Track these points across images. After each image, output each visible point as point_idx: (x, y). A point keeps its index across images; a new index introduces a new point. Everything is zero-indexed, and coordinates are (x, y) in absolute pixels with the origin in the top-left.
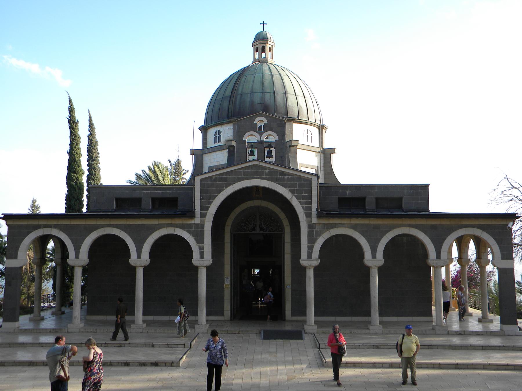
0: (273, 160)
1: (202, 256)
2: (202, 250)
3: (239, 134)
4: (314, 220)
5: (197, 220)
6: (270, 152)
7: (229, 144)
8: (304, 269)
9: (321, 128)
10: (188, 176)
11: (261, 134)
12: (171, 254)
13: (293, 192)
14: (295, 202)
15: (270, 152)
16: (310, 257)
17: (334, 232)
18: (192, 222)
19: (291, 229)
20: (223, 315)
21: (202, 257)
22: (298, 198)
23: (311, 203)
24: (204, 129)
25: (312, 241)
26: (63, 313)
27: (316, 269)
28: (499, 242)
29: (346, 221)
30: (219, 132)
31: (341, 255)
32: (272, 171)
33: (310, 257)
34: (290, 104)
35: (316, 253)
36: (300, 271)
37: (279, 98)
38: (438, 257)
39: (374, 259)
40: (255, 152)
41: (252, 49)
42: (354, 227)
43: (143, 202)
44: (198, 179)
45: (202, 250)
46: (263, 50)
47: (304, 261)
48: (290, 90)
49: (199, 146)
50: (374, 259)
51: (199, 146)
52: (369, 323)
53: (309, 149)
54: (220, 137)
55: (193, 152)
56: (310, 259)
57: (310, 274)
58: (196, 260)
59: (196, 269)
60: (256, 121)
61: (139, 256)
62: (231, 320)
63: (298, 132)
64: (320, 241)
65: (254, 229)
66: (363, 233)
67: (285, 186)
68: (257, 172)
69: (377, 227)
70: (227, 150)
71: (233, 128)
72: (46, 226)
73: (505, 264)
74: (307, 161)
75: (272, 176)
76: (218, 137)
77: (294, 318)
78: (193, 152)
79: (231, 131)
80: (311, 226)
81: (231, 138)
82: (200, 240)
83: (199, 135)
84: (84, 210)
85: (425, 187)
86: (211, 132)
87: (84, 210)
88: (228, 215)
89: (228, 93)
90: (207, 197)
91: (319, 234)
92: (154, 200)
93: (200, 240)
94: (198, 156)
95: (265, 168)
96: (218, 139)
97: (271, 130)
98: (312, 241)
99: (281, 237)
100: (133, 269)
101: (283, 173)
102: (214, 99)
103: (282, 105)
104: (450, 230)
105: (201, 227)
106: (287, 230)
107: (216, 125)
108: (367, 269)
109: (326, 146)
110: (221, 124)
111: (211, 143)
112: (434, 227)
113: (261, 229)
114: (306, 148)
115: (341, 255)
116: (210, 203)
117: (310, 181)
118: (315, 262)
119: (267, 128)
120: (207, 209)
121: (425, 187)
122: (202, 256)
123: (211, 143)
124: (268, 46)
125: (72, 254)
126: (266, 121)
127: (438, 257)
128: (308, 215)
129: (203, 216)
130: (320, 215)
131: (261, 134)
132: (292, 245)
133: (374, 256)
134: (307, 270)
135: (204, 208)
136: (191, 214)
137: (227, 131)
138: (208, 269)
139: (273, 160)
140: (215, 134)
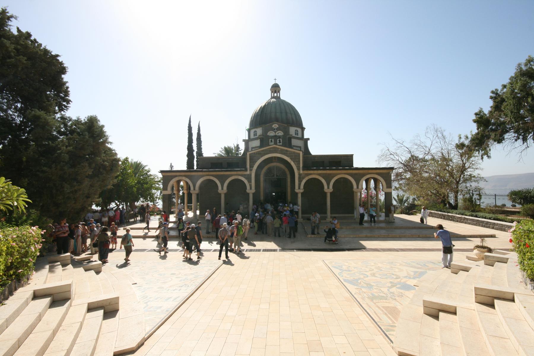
0: (281, 144)
1: (251, 189)
2: (251, 186)
3: (265, 132)
4: (301, 172)
5: (248, 172)
6: (280, 141)
8: (297, 194)
10: (242, 152)
11: (275, 132)
13: (291, 159)
14: (292, 164)
15: (280, 141)
16: (299, 188)
17: (310, 177)
21: (251, 190)
22: (294, 162)
23: (300, 164)
24: (249, 131)
28: (386, 181)
29: (316, 172)
32: (282, 150)
33: (299, 188)
35: (302, 187)
38: (358, 187)
39: (328, 189)
40: (273, 140)
41: (270, 92)
42: (319, 175)
44: (248, 154)
45: (251, 186)
47: (297, 190)
48: (288, 111)
49: (247, 138)
50: (328, 189)
51: (247, 138)
52: (326, 217)
55: (244, 140)
56: (299, 189)
58: (248, 190)
59: (248, 194)
60: (273, 126)
61: (222, 189)
64: (304, 181)
65: (274, 176)
67: (288, 156)
68: (275, 150)
69: (330, 174)
70: (259, 140)
73: (388, 190)
75: (282, 152)
78: (244, 140)
80: (300, 175)
82: (250, 181)
84: (195, 167)
85: (351, 156)
86: (252, 131)
87: (195, 167)
88: (262, 169)
89: (260, 113)
90: (253, 160)
91: (303, 178)
92: (228, 163)
93: (250, 181)
94: (246, 142)
95: (279, 148)
96: (255, 134)
97: (280, 130)
99: (285, 180)
100: (220, 194)
101: (287, 151)
104: (364, 175)
105: (250, 175)
107: (254, 128)
108: (325, 194)
109: (305, 137)
112: (356, 174)
117: (299, 154)
118: (302, 191)
119: (278, 129)
120: (253, 167)
121: (351, 156)
122: (251, 189)
123: (252, 136)
125: (192, 188)
126: (278, 126)
127: (358, 187)
129: (251, 170)
130: (303, 170)
131: (275, 132)
132: (291, 183)
133: (328, 188)
135: (251, 167)
136: (246, 170)
137: (259, 131)
138: (254, 194)
139: (281, 144)
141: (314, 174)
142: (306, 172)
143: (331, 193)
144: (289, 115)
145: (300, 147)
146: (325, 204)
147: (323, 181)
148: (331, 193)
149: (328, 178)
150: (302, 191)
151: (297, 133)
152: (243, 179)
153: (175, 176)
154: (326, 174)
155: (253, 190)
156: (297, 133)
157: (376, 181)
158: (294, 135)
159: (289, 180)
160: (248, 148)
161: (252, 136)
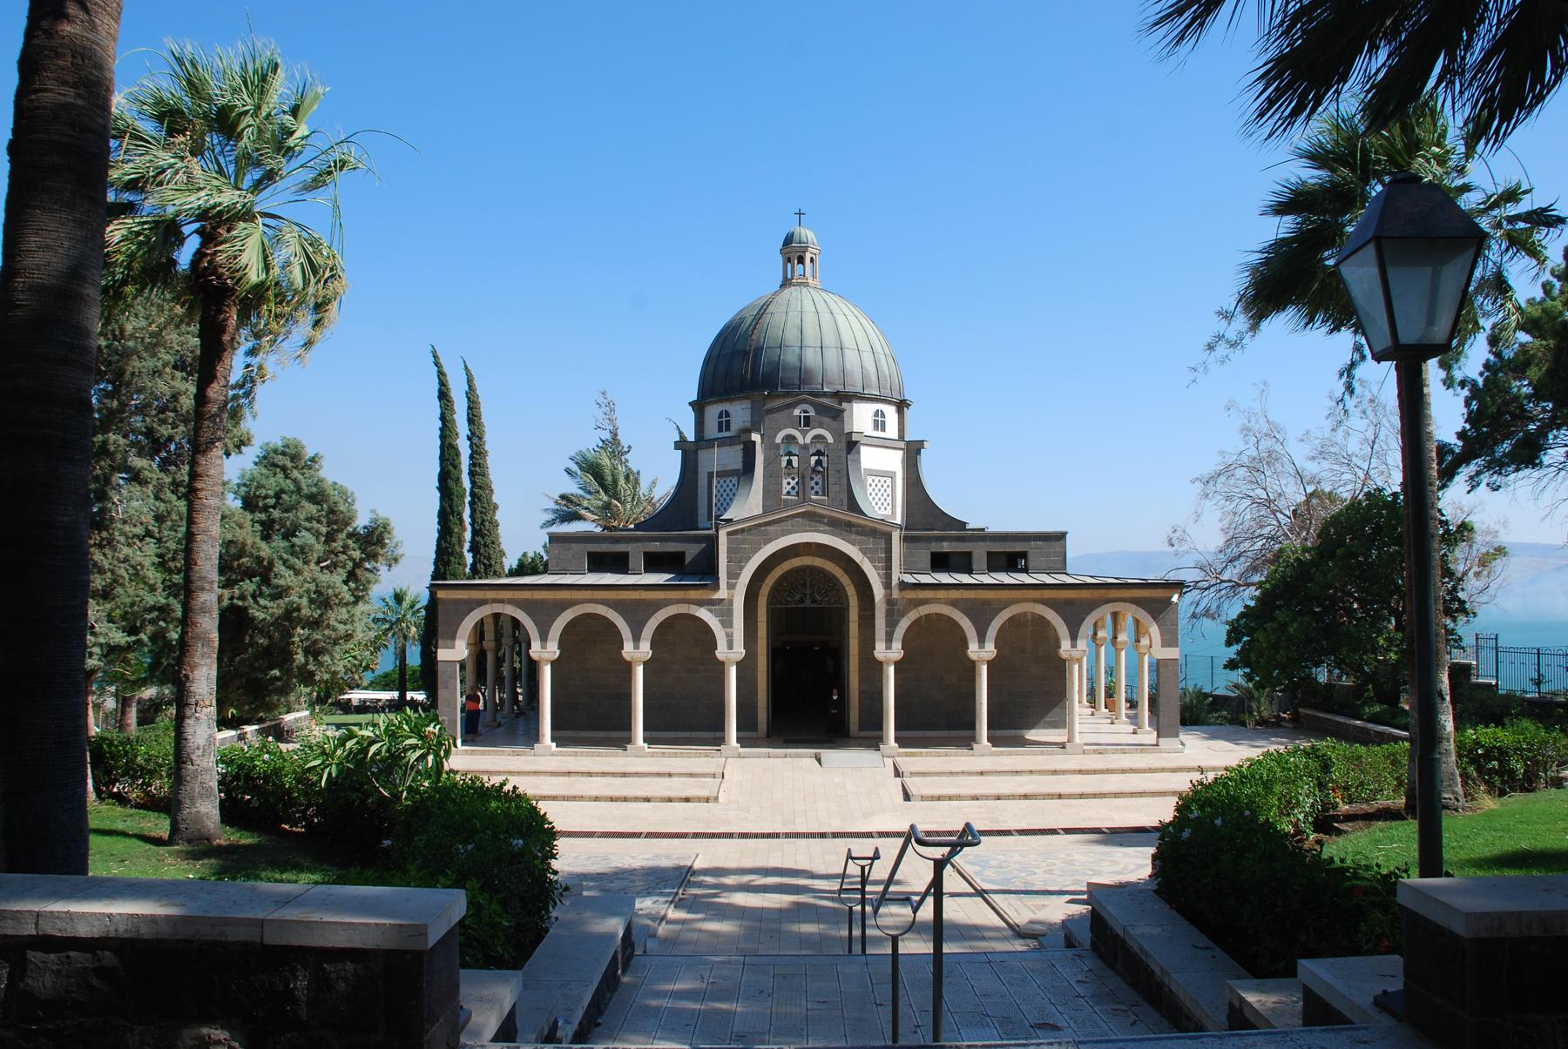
1: (730, 646)
4: (896, 594)
5: (722, 593)
7: (744, 438)
9: (902, 406)
12: (685, 645)
13: (864, 551)
17: (924, 610)
18: (716, 596)
19: (860, 599)
20: (755, 729)
21: (730, 647)
22: (872, 561)
24: (698, 407)
26: (499, 725)
29: (942, 594)
30: (727, 414)
34: (848, 366)
36: (873, 669)
37: (831, 357)
39: (981, 652)
41: (780, 259)
42: (954, 603)
43: (631, 559)
46: (801, 260)
47: (880, 651)
49: (691, 437)
53: (884, 444)
54: (728, 422)
55: (681, 444)
56: (889, 652)
58: (721, 652)
59: (723, 663)
62: (768, 736)
63: (861, 417)
66: (966, 613)
69: (986, 603)
71: (752, 409)
72: (495, 601)
74: (882, 500)
76: (724, 425)
79: (748, 412)
80: (890, 602)
82: (727, 623)
83: (690, 415)
85: (1061, 537)
86: (712, 412)
93: (727, 623)
94: (690, 452)
96: (724, 425)
97: (821, 426)
102: (715, 353)
103: (835, 370)
104: (1093, 605)
106: (853, 602)
107: (721, 401)
110: (730, 400)
111: (712, 430)
112: (1068, 602)
113: (814, 601)
114: (876, 442)
116: (741, 568)
120: (737, 576)
122: (730, 646)
124: (808, 256)
128: (887, 585)
129: (731, 587)
131: (804, 434)
135: (733, 575)
137: (740, 413)
140: (720, 416)
143: (990, 664)
144: (851, 357)
145: (892, 475)
146: (971, 695)
147: (966, 624)
148: (990, 664)
149: (981, 614)
150: (897, 652)
151: (879, 424)
152: (703, 614)
153: (482, 602)
154: (974, 601)
155: (739, 651)
156: (879, 424)
157: (1137, 622)
158: (869, 430)
159: (854, 614)
160: (696, 472)
161: (712, 430)
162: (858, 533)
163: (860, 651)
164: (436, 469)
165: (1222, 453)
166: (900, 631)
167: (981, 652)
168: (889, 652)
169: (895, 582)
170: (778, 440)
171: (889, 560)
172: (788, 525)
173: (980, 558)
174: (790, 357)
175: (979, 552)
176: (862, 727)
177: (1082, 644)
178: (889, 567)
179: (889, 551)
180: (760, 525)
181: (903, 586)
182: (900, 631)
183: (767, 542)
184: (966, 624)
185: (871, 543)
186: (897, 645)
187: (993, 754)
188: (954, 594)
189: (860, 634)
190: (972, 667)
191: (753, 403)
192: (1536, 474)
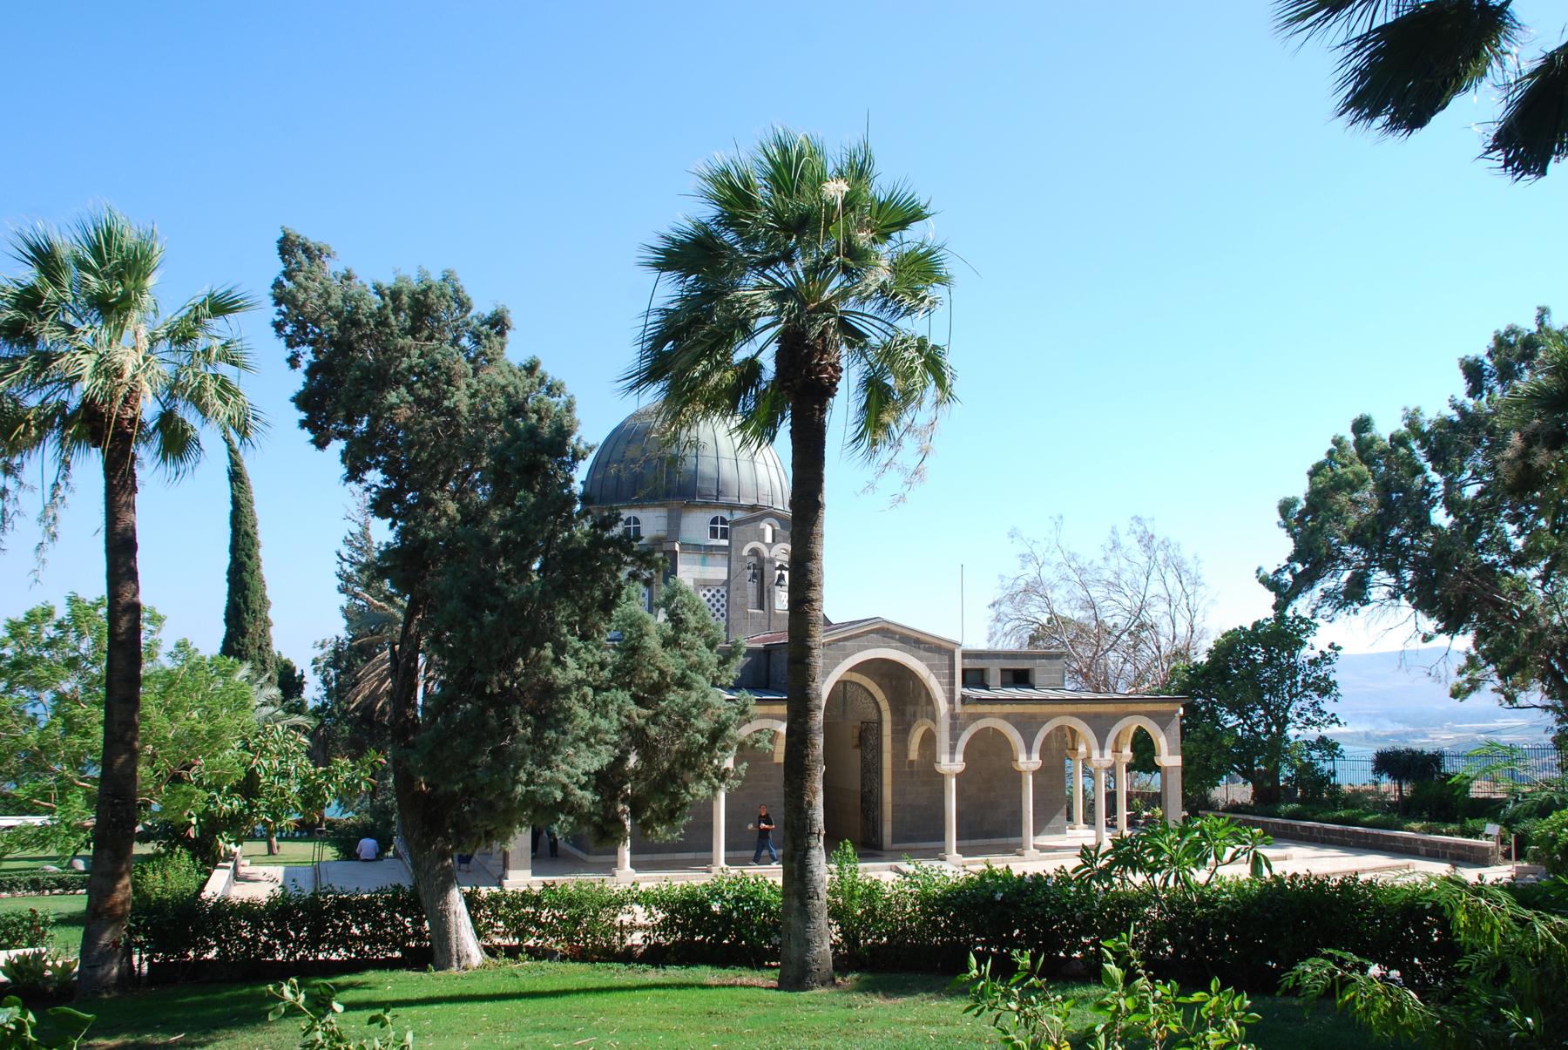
4: (959, 708)
13: (931, 667)
17: (982, 724)
22: (937, 676)
25: (954, 738)
27: (958, 776)
29: (997, 708)
30: (637, 521)
31: (988, 756)
39: (1028, 763)
42: (1006, 717)
57: (952, 784)
64: (965, 737)
66: (1017, 725)
69: (1033, 716)
71: (669, 518)
77: (896, 846)
80: (953, 716)
81: (662, 534)
98: (954, 738)
104: (1116, 718)
112: (1097, 716)
115: (988, 756)
128: (951, 701)
134: (947, 778)
141: (991, 715)
142: (971, 709)
147: (1015, 737)
148: (1035, 773)
149: (1027, 727)
150: (959, 765)
154: (1021, 715)
162: (926, 650)
163: (893, 764)
164: (225, 560)
165: (1002, 577)
166: (961, 745)
167: (1028, 763)
168: (951, 764)
169: (958, 697)
170: (745, 552)
171: (952, 676)
172: (862, 641)
173: (994, 677)
174: (706, 467)
175: (994, 670)
176: (896, 838)
177: (1108, 754)
178: (952, 683)
179: (952, 667)
180: (838, 640)
181: (964, 699)
182: (961, 745)
183: (846, 656)
184: (1015, 737)
185: (937, 659)
186: (959, 757)
187: (1041, 859)
188: (1008, 708)
189: (893, 748)
190: (1018, 776)
191: (669, 511)
192: (1366, 608)
